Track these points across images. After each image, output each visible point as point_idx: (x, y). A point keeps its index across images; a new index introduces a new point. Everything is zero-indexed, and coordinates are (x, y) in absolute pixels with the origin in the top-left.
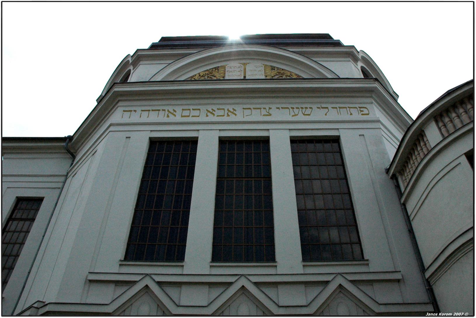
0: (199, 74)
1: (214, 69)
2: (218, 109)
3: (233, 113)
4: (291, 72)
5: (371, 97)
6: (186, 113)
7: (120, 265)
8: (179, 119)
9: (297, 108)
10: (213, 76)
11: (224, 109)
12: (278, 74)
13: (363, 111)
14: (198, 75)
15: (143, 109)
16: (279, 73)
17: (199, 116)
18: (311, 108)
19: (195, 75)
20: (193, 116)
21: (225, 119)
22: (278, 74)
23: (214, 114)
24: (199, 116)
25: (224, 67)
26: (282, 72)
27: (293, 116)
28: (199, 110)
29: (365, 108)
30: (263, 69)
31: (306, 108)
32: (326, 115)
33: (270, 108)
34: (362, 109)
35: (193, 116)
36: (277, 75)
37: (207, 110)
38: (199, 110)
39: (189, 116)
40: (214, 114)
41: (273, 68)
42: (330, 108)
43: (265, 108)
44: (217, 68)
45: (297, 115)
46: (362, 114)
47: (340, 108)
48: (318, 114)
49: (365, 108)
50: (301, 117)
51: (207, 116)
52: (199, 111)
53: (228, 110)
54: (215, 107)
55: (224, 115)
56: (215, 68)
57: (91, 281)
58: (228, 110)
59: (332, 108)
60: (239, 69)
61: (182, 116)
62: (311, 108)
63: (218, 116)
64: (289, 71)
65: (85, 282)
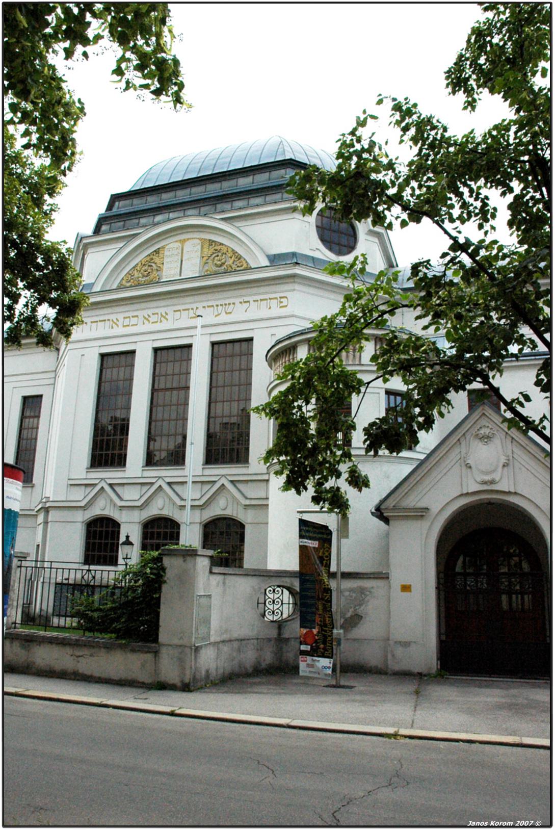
0: (141, 261)
1: (155, 253)
2: (153, 314)
3: (165, 317)
4: (228, 247)
5: (294, 282)
6: (127, 322)
7: (87, 472)
8: (120, 330)
9: (221, 305)
10: (153, 262)
11: (157, 314)
12: (214, 251)
13: (282, 302)
14: (140, 264)
15: (93, 321)
16: (216, 250)
17: (136, 325)
18: (234, 304)
19: (138, 264)
20: (132, 325)
21: (158, 327)
22: (214, 251)
23: (149, 321)
24: (136, 325)
25: (163, 247)
26: (218, 248)
27: (216, 316)
28: (137, 316)
29: (286, 297)
30: (199, 247)
31: (229, 304)
32: (246, 311)
33: (197, 308)
34: (282, 300)
35: (132, 325)
36: (213, 253)
37: (144, 317)
38: (137, 316)
39: (128, 325)
40: (149, 321)
41: (211, 242)
42: (252, 302)
43: (192, 309)
44: (157, 252)
45: (220, 314)
46: (281, 307)
47: (261, 300)
48: (240, 312)
49: (286, 297)
50: (224, 318)
51: (144, 324)
52: (137, 318)
53: (161, 314)
54: (150, 312)
55: (157, 322)
56: (155, 251)
57: (71, 485)
58: (161, 314)
59: (254, 301)
60: (175, 252)
61: (124, 326)
62: (234, 304)
63: (153, 323)
64: (226, 246)
65: (67, 486)
